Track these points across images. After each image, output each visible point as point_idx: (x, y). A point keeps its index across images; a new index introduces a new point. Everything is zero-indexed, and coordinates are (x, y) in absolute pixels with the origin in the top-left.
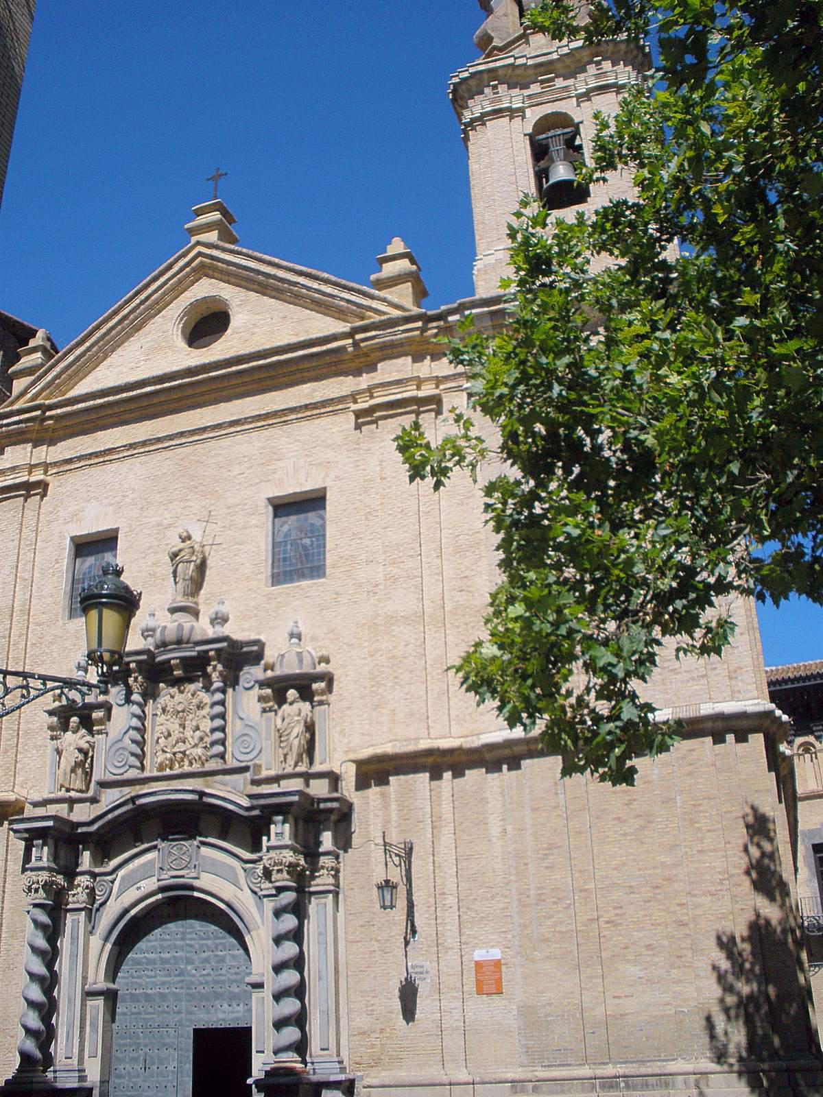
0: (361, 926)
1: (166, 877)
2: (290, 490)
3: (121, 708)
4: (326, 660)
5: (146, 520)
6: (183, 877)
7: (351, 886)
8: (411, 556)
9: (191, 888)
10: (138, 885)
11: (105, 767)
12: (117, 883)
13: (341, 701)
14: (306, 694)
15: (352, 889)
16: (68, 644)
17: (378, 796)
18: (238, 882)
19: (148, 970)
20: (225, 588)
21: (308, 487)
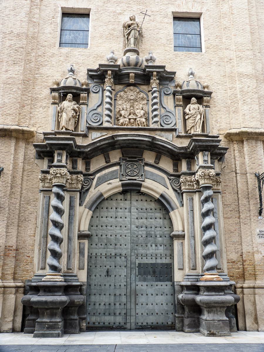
0: (231, 211)
3: (94, 94)
4: (207, 87)
5: (107, 8)
6: (135, 180)
7: (225, 192)
8: (248, 50)
11: (87, 121)
12: (95, 180)
13: (215, 107)
14: (200, 100)
15: (225, 193)
17: (237, 151)
18: (166, 184)
19: (108, 226)
20: (152, 47)
21: (193, 11)
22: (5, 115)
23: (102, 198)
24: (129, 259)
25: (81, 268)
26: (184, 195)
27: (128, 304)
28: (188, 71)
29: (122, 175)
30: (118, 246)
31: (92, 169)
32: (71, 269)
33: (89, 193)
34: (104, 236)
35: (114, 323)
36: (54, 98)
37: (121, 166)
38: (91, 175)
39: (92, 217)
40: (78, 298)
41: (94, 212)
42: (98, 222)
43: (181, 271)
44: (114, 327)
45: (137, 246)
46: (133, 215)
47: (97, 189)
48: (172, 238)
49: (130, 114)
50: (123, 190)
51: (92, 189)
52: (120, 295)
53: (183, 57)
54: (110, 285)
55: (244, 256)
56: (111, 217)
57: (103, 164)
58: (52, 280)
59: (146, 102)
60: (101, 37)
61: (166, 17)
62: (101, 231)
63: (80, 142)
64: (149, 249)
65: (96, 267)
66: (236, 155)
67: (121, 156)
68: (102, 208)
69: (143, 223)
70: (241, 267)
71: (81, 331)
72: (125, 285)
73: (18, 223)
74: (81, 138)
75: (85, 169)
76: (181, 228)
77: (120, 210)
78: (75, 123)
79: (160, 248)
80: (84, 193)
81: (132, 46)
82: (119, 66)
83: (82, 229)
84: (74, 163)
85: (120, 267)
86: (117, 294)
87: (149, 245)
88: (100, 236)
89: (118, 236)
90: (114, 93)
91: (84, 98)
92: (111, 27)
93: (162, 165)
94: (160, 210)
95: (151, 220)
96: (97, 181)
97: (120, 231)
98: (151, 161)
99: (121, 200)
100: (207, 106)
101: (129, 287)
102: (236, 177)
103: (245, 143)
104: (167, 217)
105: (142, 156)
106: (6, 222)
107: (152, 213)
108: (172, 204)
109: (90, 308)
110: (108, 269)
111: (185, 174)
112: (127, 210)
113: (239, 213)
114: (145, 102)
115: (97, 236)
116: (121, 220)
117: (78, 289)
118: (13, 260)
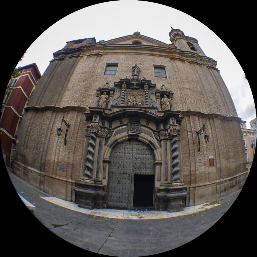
1: (130, 132)
2: (158, 65)
3: (117, 93)
4: (171, 91)
6: (136, 133)
7: (182, 140)
9: (138, 136)
10: (121, 134)
14: (168, 97)
16: (104, 79)
22: (75, 101)
23: (117, 142)
24: (131, 175)
25: (104, 178)
26: (162, 142)
27: (130, 198)
28: (161, 85)
29: (129, 130)
30: (125, 168)
31: (113, 127)
32: (98, 178)
33: (110, 139)
34: (117, 163)
35: (122, 206)
36: (98, 94)
37: (128, 126)
38: (112, 130)
39: (111, 152)
40: (102, 193)
41: (112, 149)
42: (114, 155)
43: (159, 182)
44: (122, 207)
45: (135, 168)
46: (134, 152)
47: (115, 137)
48: (155, 164)
49: (134, 101)
50: (129, 138)
51: (112, 137)
52: (125, 193)
53: (159, 80)
54: (120, 188)
55: (191, 172)
56: (122, 153)
57: (119, 124)
58: (86, 182)
59: (142, 96)
60: (122, 72)
61: (151, 66)
62: (116, 160)
63: (107, 112)
64: (142, 171)
65: (112, 178)
66: (187, 122)
67: (128, 121)
68: (117, 148)
69: (139, 157)
70: (190, 178)
71: (103, 208)
72: (128, 189)
73: (74, 152)
74: (108, 111)
75: (109, 126)
76: (160, 159)
77: (127, 149)
78: (106, 105)
79: (148, 170)
80: (108, 139)
81: (136, 74)
82: (129, 80)
83: (105, 157)
84: (103, 123)
85: (126, 179)
86: (123, 193)
87: (142, 168)
88: (115, 162)
89: (125, 163)
90: (126, 92)
91: (112, 94)
92: (126, 68)
93: (150, 126)
94: (149, 150)
95: (143, 155)
96: (115, 133)
97: (127, 161)
98: (145, 124)
99: (128, 144)
100: (171, 99)
101: (130, 189)
102: (187, 133)
103: (190, 117)
104: (152, 154)
105: (140, 120)
106: (68, 150)
107: (144, 151)
108: (155, 146)
109: (109, 198)
110: (119, 180)
111: (162, 130)
112: (131, 149)
113: (189, 151)
114: (142, 96)
115: (113, 162)
116: (127, 154)
117: (103, 188)
118: (71, 170)
